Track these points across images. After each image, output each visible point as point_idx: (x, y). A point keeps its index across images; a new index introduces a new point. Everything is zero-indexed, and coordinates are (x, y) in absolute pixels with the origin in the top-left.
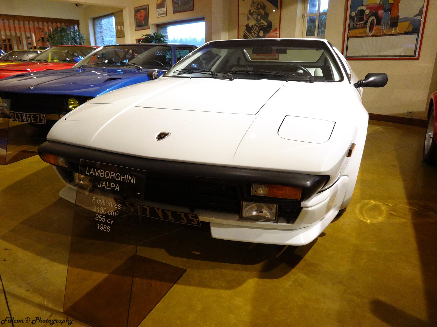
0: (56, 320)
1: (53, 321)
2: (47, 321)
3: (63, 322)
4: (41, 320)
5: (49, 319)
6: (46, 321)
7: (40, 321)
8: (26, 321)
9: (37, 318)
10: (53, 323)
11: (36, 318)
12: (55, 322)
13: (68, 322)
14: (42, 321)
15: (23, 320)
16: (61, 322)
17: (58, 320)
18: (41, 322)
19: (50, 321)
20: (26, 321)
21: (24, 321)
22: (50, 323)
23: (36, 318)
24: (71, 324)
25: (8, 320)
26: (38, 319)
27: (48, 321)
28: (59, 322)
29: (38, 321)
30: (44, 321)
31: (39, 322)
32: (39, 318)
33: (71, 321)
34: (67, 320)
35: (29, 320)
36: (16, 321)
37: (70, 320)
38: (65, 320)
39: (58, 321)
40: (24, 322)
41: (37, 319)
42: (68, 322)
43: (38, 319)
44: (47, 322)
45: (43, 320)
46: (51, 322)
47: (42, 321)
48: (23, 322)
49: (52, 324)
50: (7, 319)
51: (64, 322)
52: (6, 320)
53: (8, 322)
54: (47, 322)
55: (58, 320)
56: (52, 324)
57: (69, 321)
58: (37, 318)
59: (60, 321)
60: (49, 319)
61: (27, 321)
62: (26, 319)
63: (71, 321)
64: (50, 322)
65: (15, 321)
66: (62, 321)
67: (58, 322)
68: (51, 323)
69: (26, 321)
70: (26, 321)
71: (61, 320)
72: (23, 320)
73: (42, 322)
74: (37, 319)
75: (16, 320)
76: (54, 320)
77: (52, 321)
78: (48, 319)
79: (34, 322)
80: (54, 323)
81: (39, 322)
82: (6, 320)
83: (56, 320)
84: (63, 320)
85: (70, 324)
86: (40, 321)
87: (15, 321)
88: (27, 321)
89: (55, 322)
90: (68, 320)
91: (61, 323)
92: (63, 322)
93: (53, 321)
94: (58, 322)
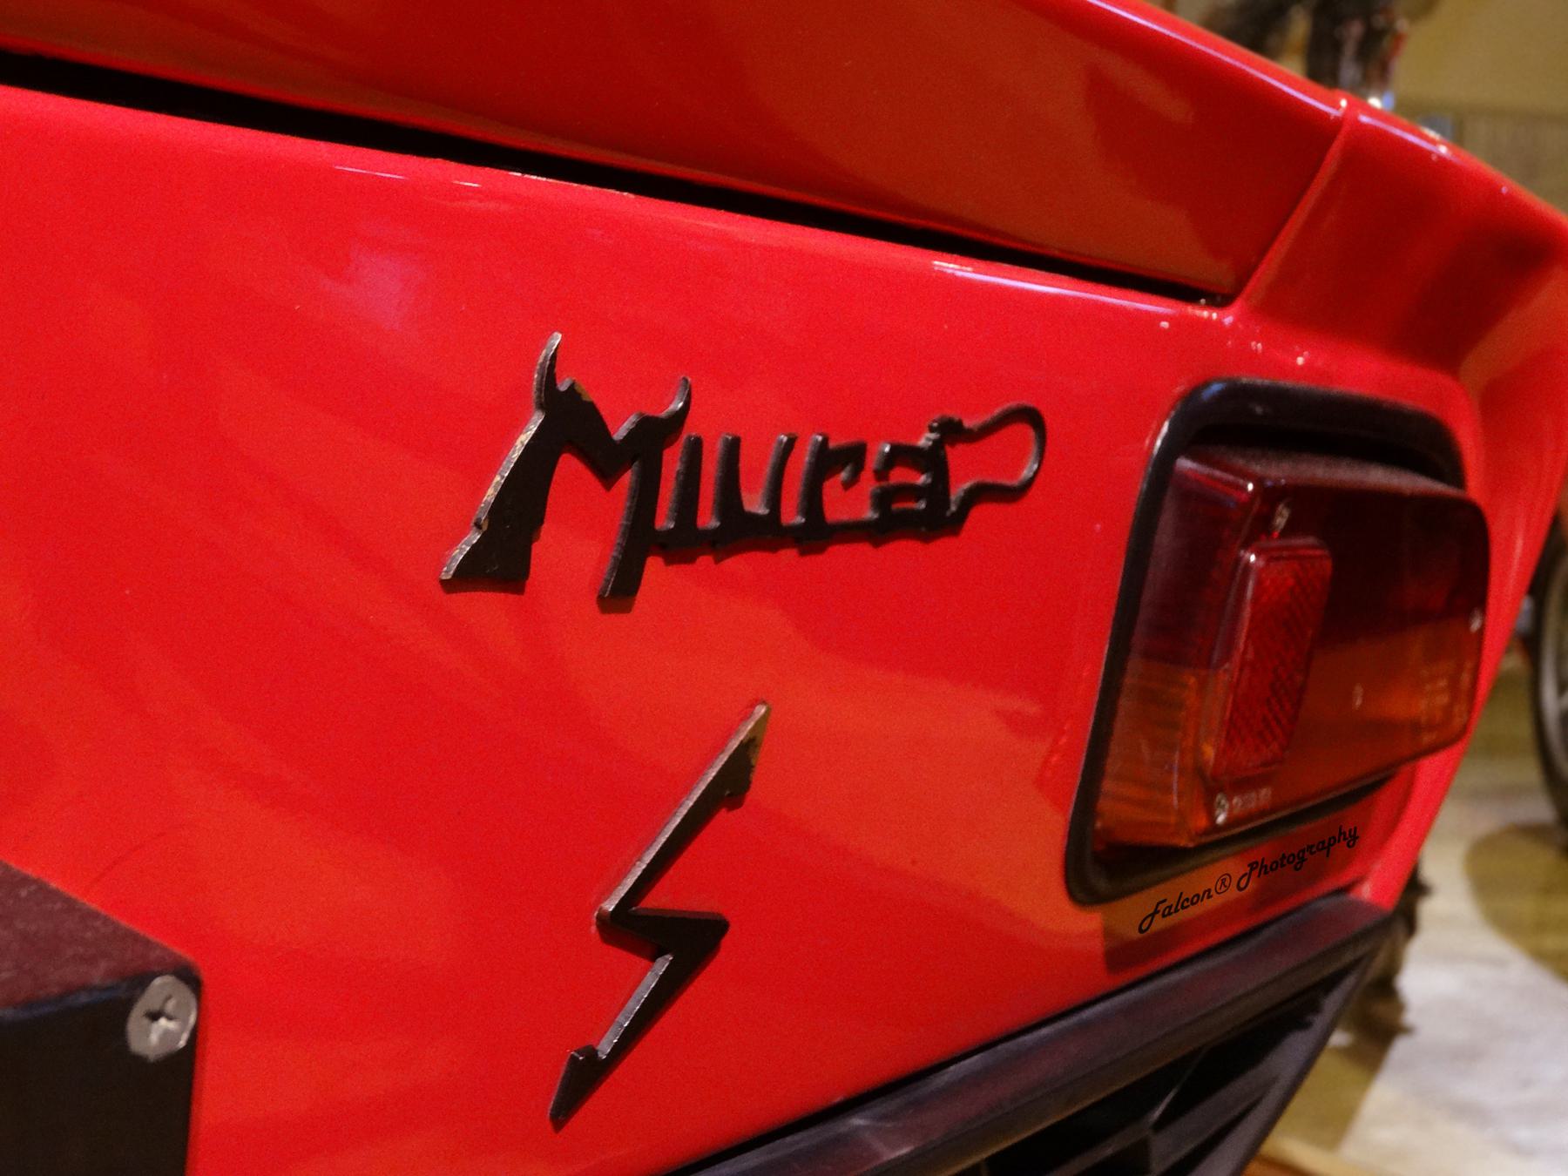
0: (1308, 847)
1: (1301, 855)
2: (1282, 863)
3: (1330, 845)
4: (1266, 866)
5: (1287, 855)
6: (1280, 862)
7: (1263, 870)
10: (1302, 860)
11: (1249, 868)
14: (1268, 868)
15: (1209, 890)
16: (1324, 848)
17: (1313, 846)
19: (1291, 859)
20: (1219, 891)
21: (1213, 892)
24: (1355, 842)
25: (1162, 910)
27: (1285, 861)
28: (1318, 850)
30: (1274, 866)
33: (1352, 833)
34: (1340, 833)
35: (1227, 883)
36: (1189, 903)
37: (1350, 831)
38: (1334, 837)
39: (1314, 850)
40: (1212, 896)
41: (1252, 869)
42: (1345, 839)
43: (1255, 869)
44: (1283, 866)
46: (1297, 861)
47: (1268, 868)
50: (1161, 907)
51: (1334, 844)
52: (1156, 912)
54: (1284, 865)
55: (1313, 846)
57: (1347, 835)
61: (1223, 889)
63: (1352, 833)
64: (1293, 861)
65: (1186, 904)
66: (1326, 845)
67: (1315, 852)
68: (1298, 863)
70: (1218, 887)
72: (1209, 890)
74: (1252, 869)
76: (1303, 851)
78: (1284, 855)
81: (1259, 876)
83: (1310, 847)
84: (1330, 839)
86: (1263, 870)
87: (1186, 904)
88: (1223, 889)
90: (1345, 833)
91: (1326, 851)
92: (1330, 845)
93: (1301, 855)
94: (1315, 852)
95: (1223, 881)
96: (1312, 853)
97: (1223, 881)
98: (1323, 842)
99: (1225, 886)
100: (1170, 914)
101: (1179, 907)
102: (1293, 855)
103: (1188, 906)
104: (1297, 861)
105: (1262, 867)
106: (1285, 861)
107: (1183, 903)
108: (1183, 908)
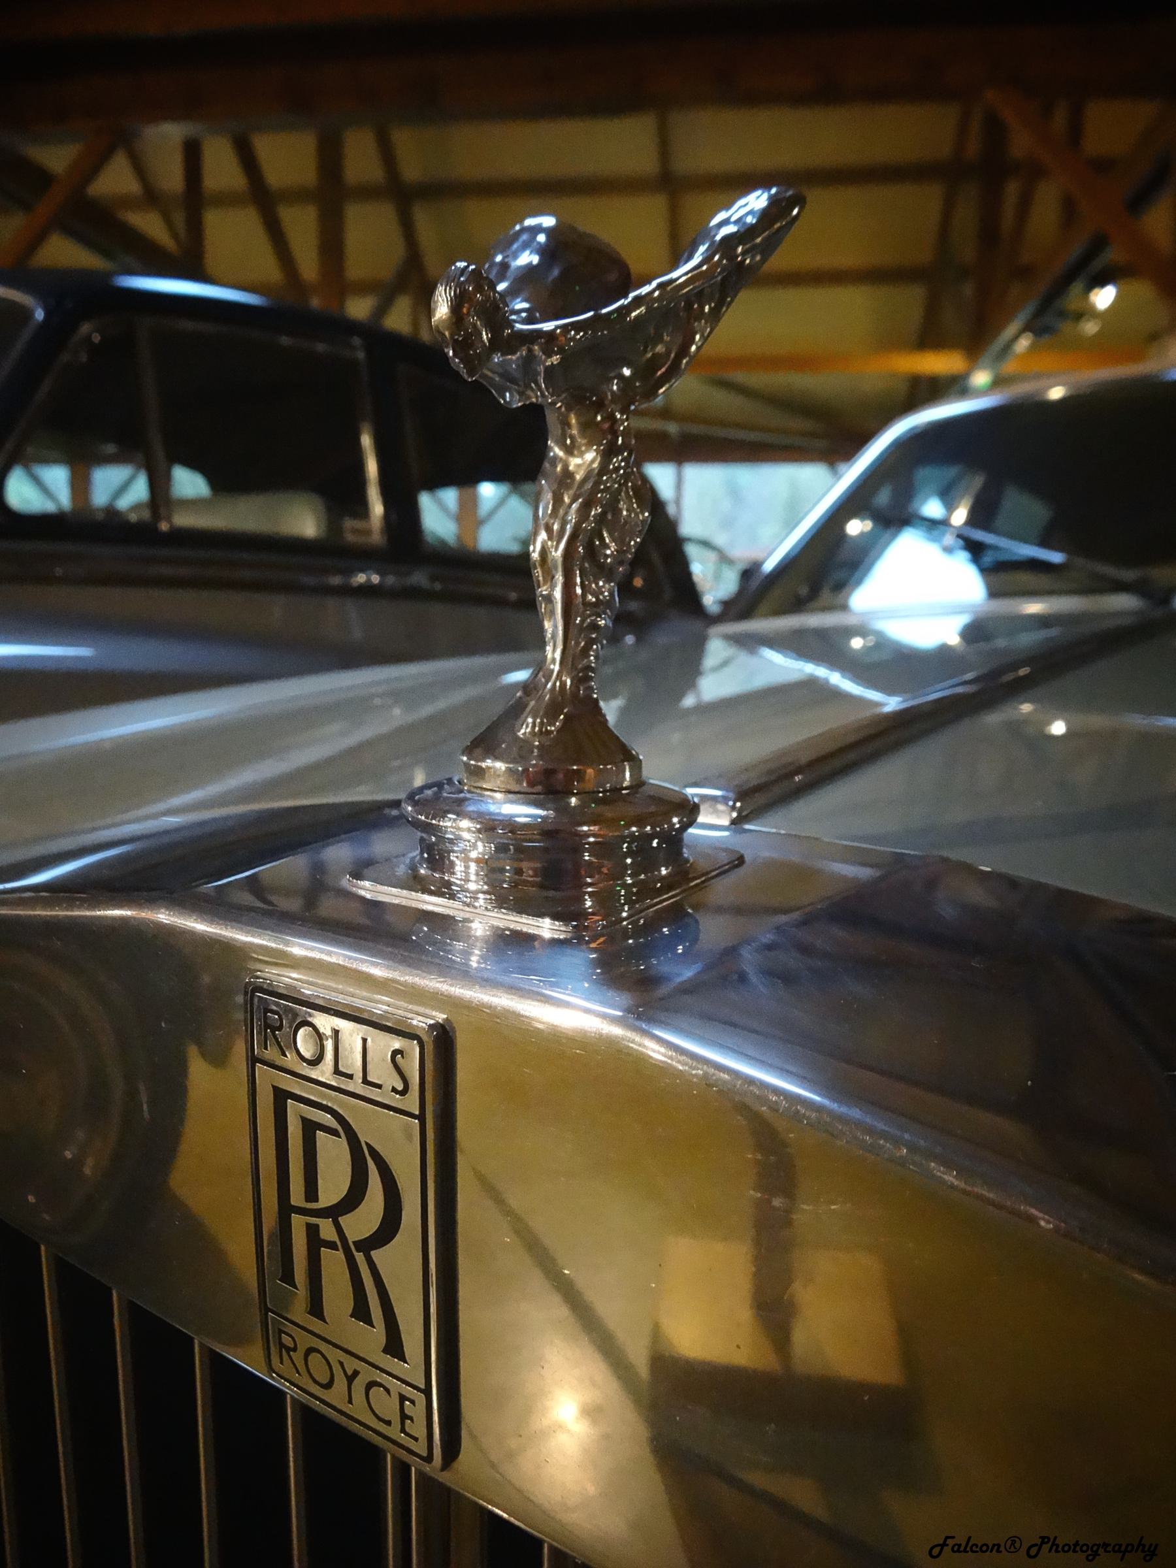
0: (1104, 1544)
1: (1095, 1549)
3: (1126, 1551)
4: (1058, 1546)
5: (1081, 1543)
6: (1072, 1547)
8: (1010, 1548)
9: (1042, 1538)
12: (1101, 1551)
13: (1143, 1551)
14: (1060, 1549)
15: (999, 1545)
16: (1119, 1551)
17: (1110, 1545)
18: (1057, 1551)
20: (1008, 1547)
21: (1002, 1548)
22: (1086, 1554)
23: (1040, 1537)
26: (1046, 1540)
29: (1046, 1547)
31: (1050, 1551)
32: (1049, 1538)
33: (1152, 1549)
34: (1140, 1544)
35: (1017, 1545)
37: (1151, 1545)
38: (1133, 1545)
39: (1109, 1548)
44: (1075, 1551)
45: (1063, 1544)
46: (1089, 1552)
48: (998, 1551)
49: (1090, 1558)
50: (949, 1541)
52: (944, 1545)
53: (953, 1551)
55: (1110, 1545)
56: (1090, 1558)
58: (1044, 1540)
59: (1117, 1548)
60: (1081, 1543)
62: (1009, 1542)
65: (974, 1548)
66: (1123, 1549)
69: (1010, 1548)
71: (1120, 1546)
72: (999, 1545)
73: (1059, 1552)
75: (976, 1545)
76: (1099, 1546)
77: (1090, 1546)
78: (1077, 1542)
79: (1033, 1551)
80: (1099, 1555)
82: (944, 1545)
83: (1106, 1545)
85: (1148, 1558)
87: (974, 1548)
88: (1012, 1549)
89: (1101, 1551)
93: (1095, 1549)
94: (1109, 1552)
95: (1013, 1542)
96: (1106, 1551)
97: (1013, 1542)
98: (1120, 1546)
99: (1015, 1548)
100: (958, 1551)
101: (968, 1549)
102: (1087, 1545)
103: (977, 1552)
104: (1089, 1552)
105: (1053, 1544)
106: (1078, 1548)
107: (973, 1545)
108: (973, 1551)
